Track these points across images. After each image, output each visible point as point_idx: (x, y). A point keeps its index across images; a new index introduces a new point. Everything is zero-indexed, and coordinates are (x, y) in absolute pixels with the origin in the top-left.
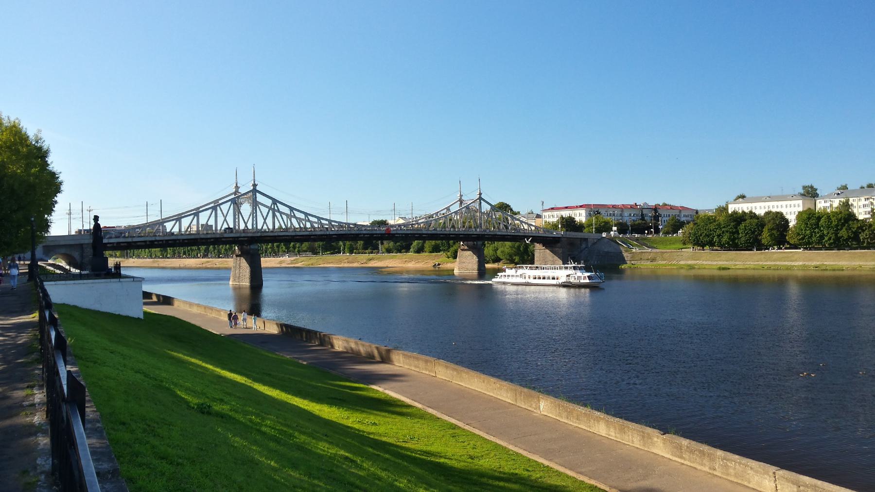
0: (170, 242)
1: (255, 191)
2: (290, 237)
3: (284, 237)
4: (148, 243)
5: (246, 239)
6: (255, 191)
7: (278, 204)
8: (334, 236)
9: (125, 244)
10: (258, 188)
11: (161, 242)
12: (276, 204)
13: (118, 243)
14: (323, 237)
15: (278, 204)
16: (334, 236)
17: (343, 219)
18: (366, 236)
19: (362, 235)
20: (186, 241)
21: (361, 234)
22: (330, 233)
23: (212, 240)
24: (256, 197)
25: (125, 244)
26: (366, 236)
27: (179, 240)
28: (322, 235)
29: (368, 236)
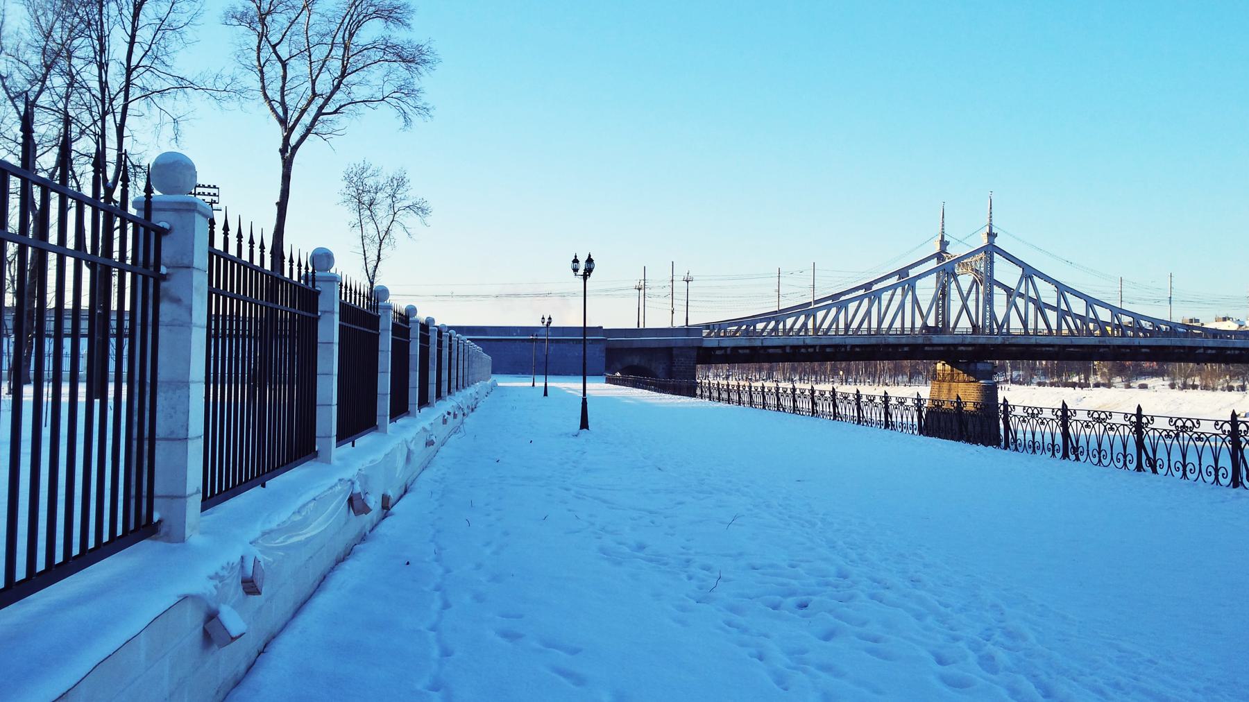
0: (828, 350)
1: (991, 250)
2: (1056, 349)
3: (1044, 349)
4: (788, 350)
5: (970, 349)
6: (991, 250)
7: (1036, 279)
8: (1143, 350)
9: (748, 351)
10: (997, 242)
11: (810, 350)
12: (1031, 278)
13: (735, 349)
14: (1123, 350)
15: (1036, 279)
16: (1143, 350)
17: (1161, 313)
18: (1209, 351)
19: (1201, 351)
20: (858, 349)
21: (1200, 348)
22: (1141, 344)
23: (906, 349)
24: (992, 262)
25: (748, 351)
26: (1209, 351)
27: (845, 346)
28: (1119, 347)
29: (1214, 352)
